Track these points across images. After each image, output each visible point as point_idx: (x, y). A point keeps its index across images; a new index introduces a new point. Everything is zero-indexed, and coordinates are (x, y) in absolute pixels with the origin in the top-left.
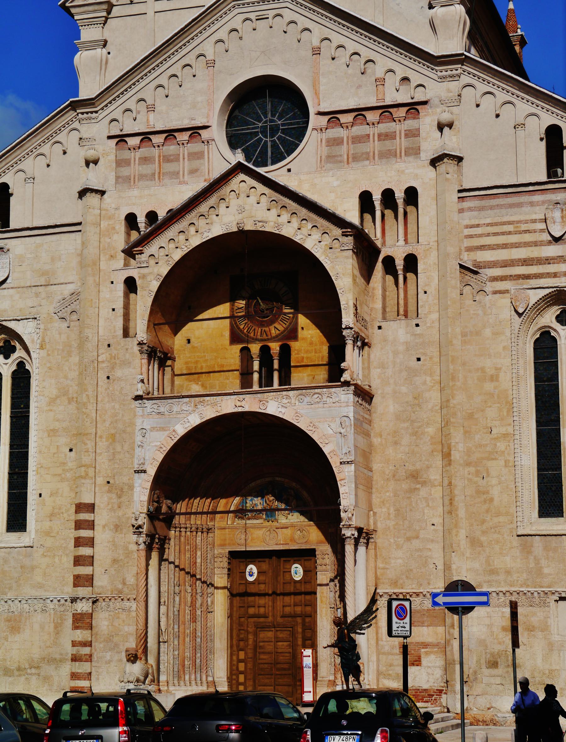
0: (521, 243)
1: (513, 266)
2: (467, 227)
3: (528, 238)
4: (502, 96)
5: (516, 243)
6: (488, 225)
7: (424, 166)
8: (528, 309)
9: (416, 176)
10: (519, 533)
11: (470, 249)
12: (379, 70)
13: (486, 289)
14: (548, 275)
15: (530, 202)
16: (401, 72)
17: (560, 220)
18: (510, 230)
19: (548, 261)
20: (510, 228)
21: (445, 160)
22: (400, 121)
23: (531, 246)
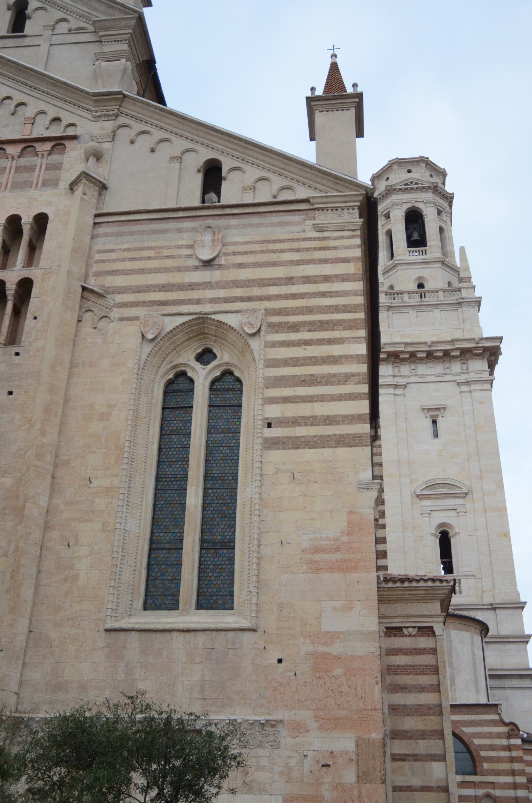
0: (161, 268)
1: (149, 291)
2: (99, 252)
3: (169, 263)
4: (158, 134)
5: (155, 268)
6: (125, 250)
7: (61, 194)
8: (161, 337)
9: (50, 204)
10: (109, 626)
11: (98, 274)
12: (30, 111)
13: (111, 315)
14: (190, 302)
15: (178, 229)
16: (52, 113)
17: (210, 243)
18: (150, 255)
19: (192, 287)
20: (152, 253)
21: (84, 180)
22: (43, 155)
23: (174, 272)
